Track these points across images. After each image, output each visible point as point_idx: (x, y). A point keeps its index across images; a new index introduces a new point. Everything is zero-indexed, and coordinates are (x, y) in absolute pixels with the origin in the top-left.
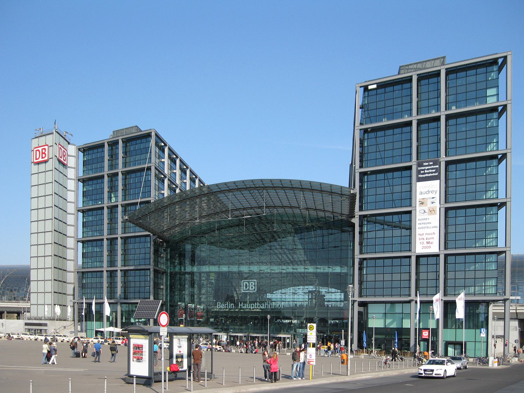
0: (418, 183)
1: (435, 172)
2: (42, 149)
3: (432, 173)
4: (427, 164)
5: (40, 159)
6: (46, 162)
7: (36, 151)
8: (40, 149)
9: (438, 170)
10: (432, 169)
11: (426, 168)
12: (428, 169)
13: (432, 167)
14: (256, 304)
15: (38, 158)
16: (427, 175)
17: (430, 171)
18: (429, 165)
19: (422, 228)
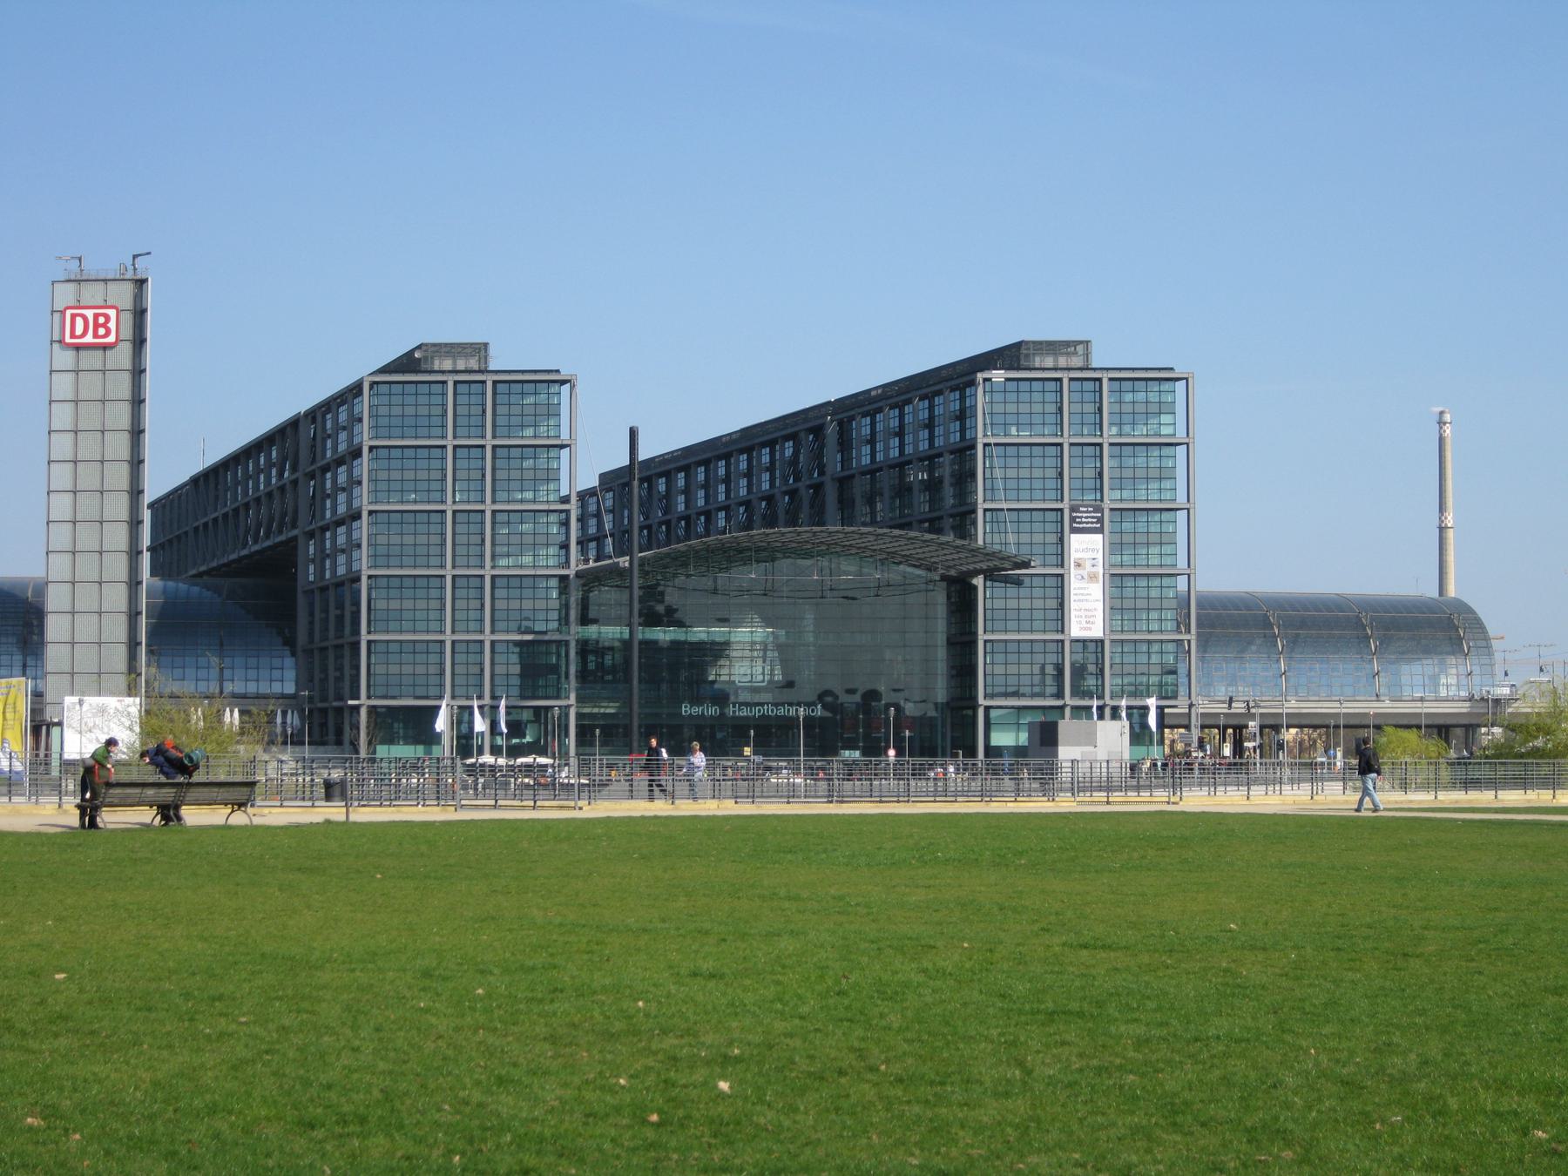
0: (1073, 536)
1: (1096, 523)
2: (96, 316)
3: (1092, 523)
4: (1085, 509)
5: (89, 339)
6: (105, 347)
7: (73, 317)
8: (90, 314)
9: (1100, 520)
10: (1093, 517)
11: (1085, 515)
12: (1086, 517)
13: (1093, 514)
14: (766, 707)
15: (79, 331)
16: (1085, 525)
17: (1090, 520)
18: (1087, 512)
19: (1079, 600)
